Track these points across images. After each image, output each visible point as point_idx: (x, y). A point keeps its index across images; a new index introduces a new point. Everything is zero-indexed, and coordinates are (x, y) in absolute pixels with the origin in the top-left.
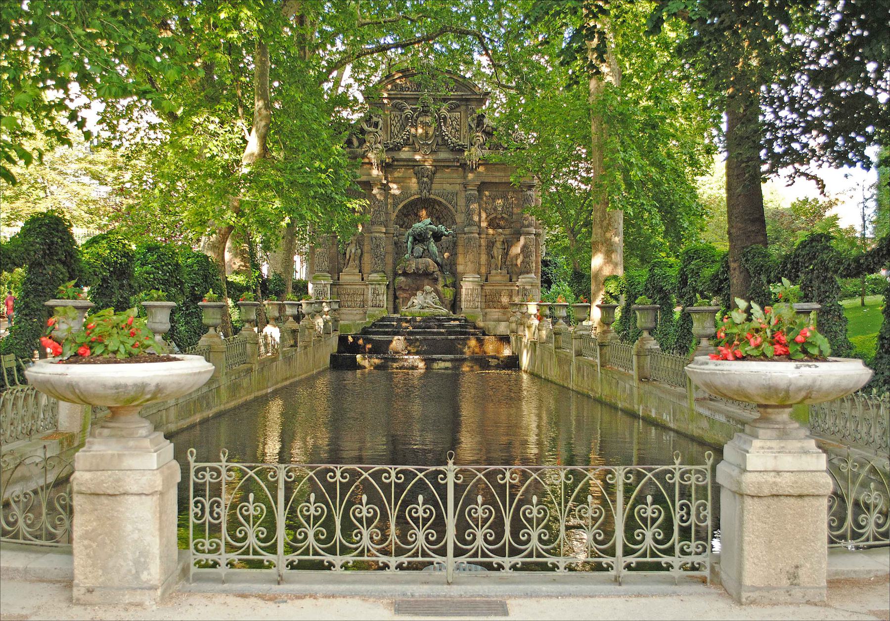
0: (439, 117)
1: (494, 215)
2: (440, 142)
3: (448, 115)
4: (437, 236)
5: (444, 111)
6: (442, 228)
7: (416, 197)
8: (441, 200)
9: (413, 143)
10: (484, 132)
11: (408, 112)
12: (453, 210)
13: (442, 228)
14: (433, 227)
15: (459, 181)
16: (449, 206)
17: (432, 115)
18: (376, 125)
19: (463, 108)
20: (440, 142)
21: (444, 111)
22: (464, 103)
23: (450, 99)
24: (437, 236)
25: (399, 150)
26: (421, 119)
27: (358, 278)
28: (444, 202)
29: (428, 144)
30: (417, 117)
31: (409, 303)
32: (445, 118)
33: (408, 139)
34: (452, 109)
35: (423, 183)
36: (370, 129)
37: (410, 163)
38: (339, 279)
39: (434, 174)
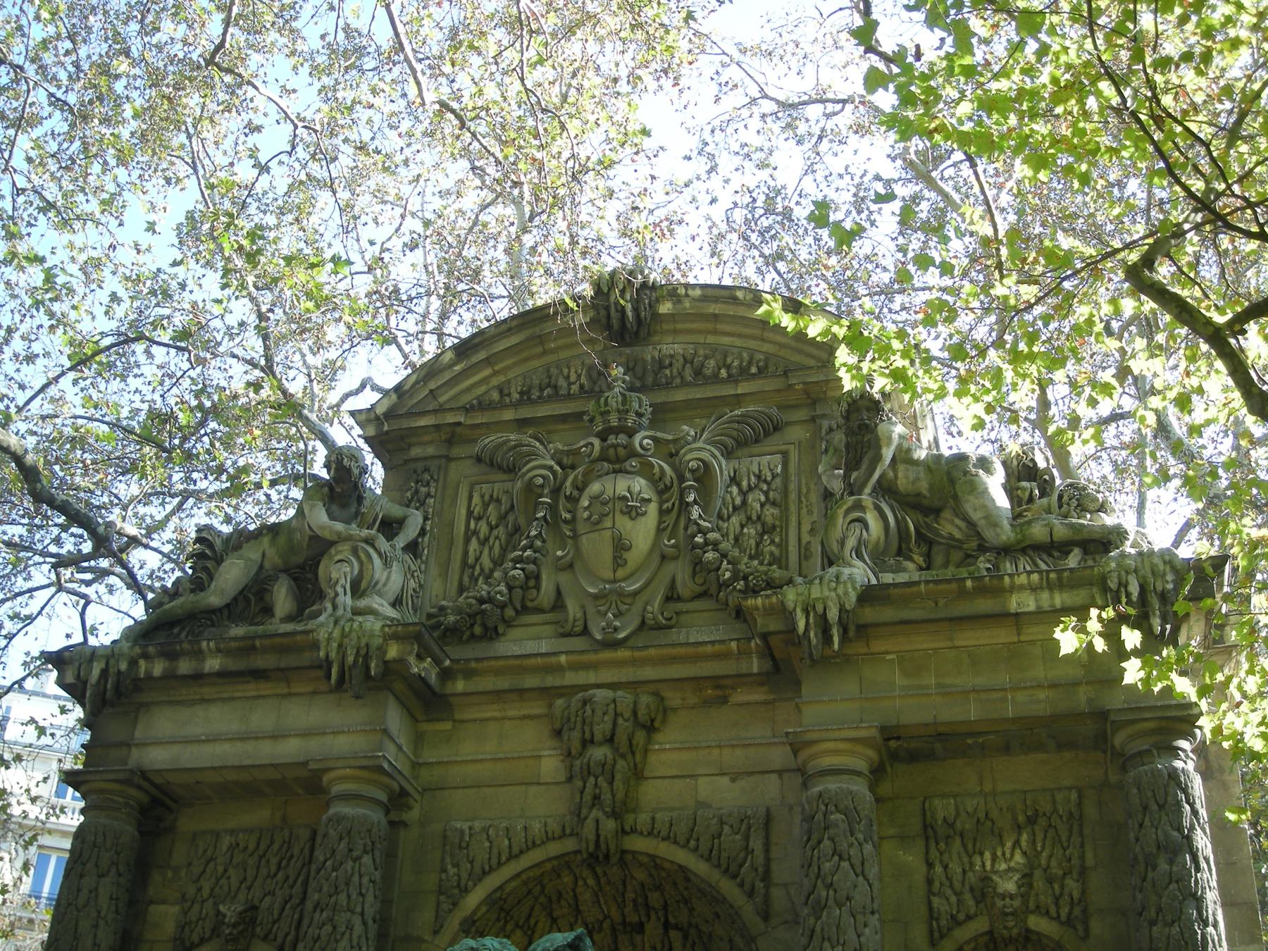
1: (980, 925)
2: (686, 586)
3: (722, 468)
5: (700, 451)
7: (554, 849)
8: (682, 856)
9: (558, 604)
10: (886, 489)
11: (541, 466)
12: (748, 910)
15: (779, 756)
16: (728, 888)
17: (646, 470)
19: (798, 433)
20: (686, 586)
21: (700, 451)
25: (492, 634)
26: (595, 487)
28: (700, 867)
29: (621, 594)
30: (581, 488)
33: (538, 577)
34: (742, 443)
35: (587, 772)
37: (531, 682)
39: (650, 728)
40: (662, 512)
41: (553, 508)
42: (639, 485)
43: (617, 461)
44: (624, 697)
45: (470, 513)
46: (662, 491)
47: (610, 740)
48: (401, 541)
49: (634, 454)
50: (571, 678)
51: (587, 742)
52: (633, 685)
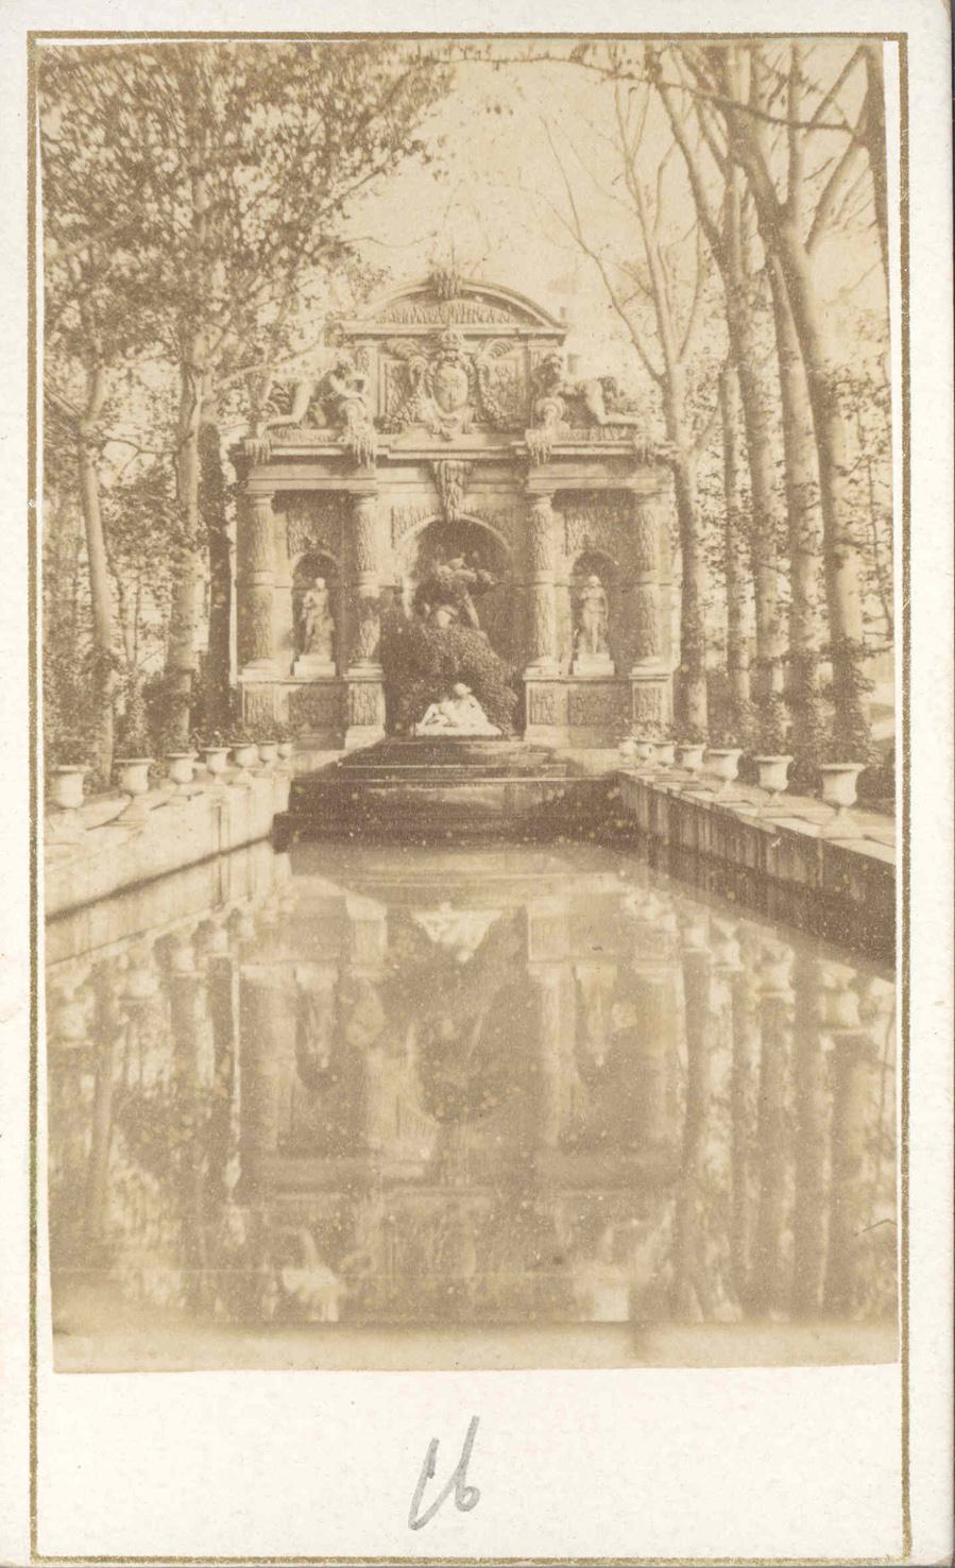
0: (477, 371)
4: (478, 589)
6: (487, 576)
7: (432, 519)
10: (561, 394)
13: (487, 576)
14: (470, 574)
17: (463, 368)
18: (360, 384)
22: (522, 344)
23: (496, 336)
24: (478, 589)
27: (329, 670)
28: (486, 525)
29: (455, 420)
31: (428, 716)
32: (487, 373)
36: (351, 393)
38: (292, 671)
40: (470, 386)
41: (425, 381)
42: (463, 376)
43: (453, 361)
44: (462, 464)
45: (386, 374)
46: (469, 377)
47: (456, 480)
48: (365, 389)
49: (457, 359)
50: (442, 456)
51: (448, 481)
52: (464, 460)
